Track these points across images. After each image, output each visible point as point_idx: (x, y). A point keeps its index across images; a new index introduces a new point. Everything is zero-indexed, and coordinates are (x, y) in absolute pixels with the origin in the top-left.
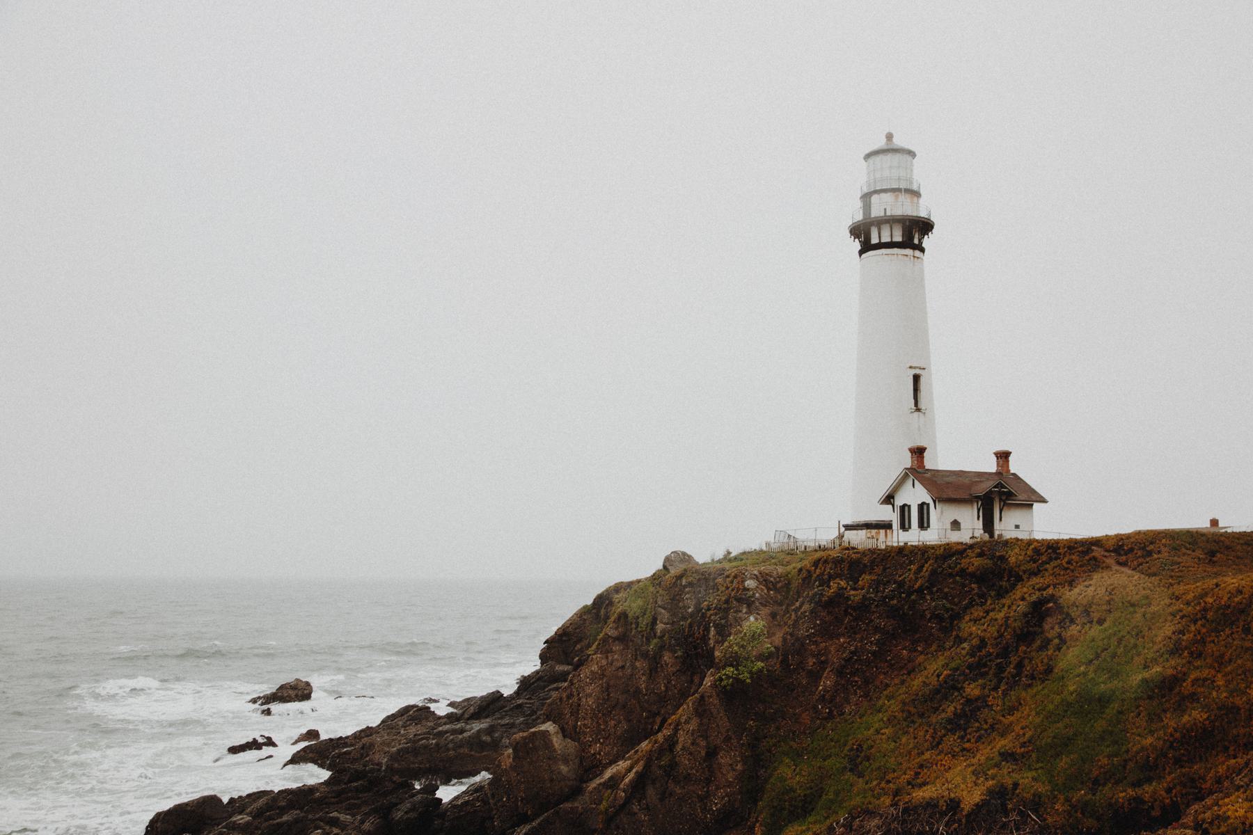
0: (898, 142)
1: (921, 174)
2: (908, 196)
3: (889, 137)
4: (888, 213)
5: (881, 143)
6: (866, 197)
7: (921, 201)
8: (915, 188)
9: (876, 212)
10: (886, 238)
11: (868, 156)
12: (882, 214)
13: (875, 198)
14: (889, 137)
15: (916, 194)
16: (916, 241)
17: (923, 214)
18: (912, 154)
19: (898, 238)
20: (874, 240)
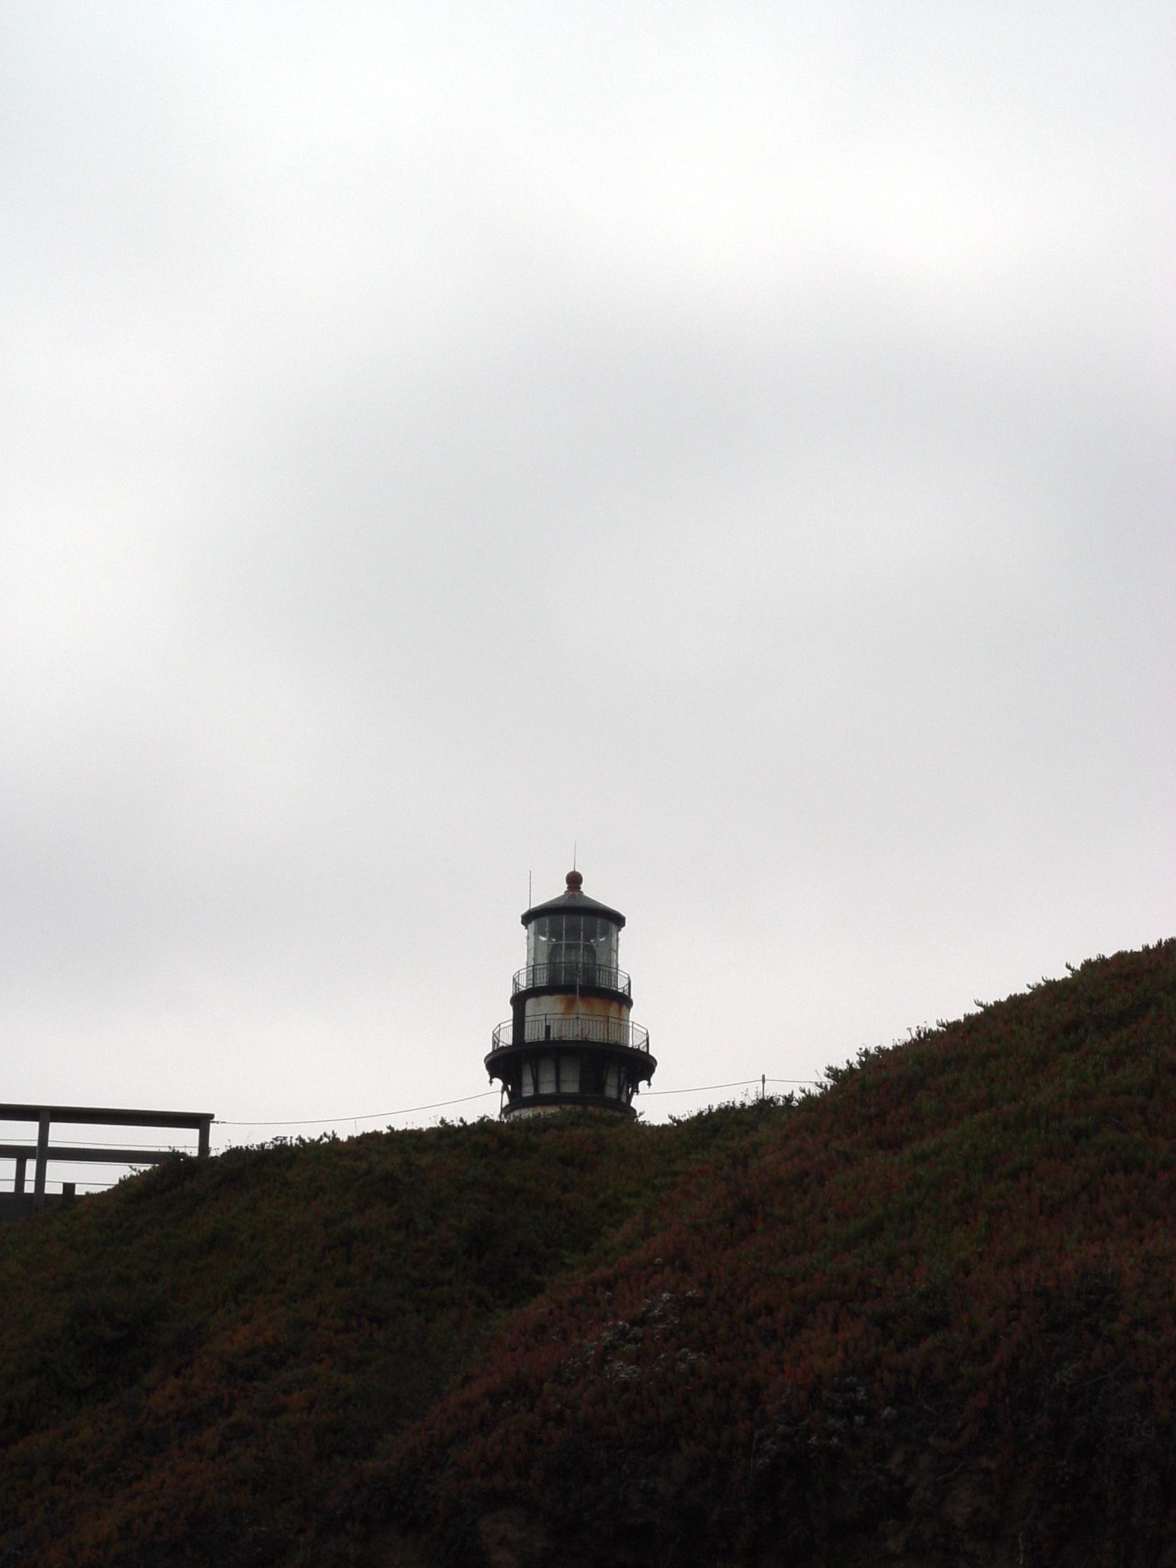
0: (591, 890)
1: (634, 959)
2: (598, 1005)
3: (574, 880)
4: (554, 1035)
5: (556, 890)
6: (519, 1001)
7: (634, 1015)
8: (621, 985)
9: (533, 1033)
10: (547, 1089)
11: (527, 919)
12: (542, 1037)
13: (530, 1004)
14: (574, 880)
15: (625, 1001)
16: (611, 1092)
17: (634, 1040)
18: (618, 920)
19: (571, 1087)
20: (528, 1091)
